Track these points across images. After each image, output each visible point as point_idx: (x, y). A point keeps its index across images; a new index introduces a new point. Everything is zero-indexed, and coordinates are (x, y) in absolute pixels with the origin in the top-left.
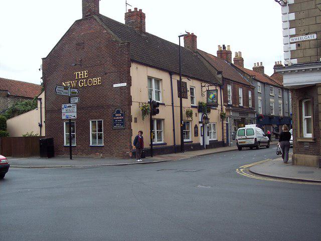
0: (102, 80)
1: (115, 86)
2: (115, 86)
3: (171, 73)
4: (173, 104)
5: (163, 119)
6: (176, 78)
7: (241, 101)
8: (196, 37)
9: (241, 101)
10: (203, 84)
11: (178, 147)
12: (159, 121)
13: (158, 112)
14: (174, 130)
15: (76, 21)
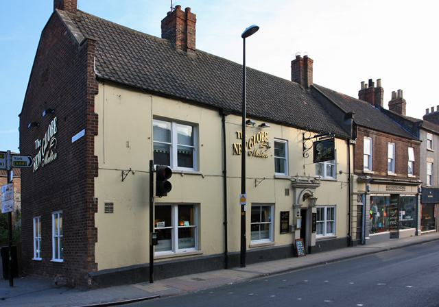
0: (86, 133)
1: (74, 139)
2: (74, 139)
3: (223, 112)
4: (224, 172)
5: (199, 204)
6: (234, 121)
7: (37, 251)
8: (312, 62)
9: (37, 251)
10: (308, 134)
11: (234, 255)
12: (188, 210)
13: (168, 187)
14: (225, 224)
15: (42, 32)
